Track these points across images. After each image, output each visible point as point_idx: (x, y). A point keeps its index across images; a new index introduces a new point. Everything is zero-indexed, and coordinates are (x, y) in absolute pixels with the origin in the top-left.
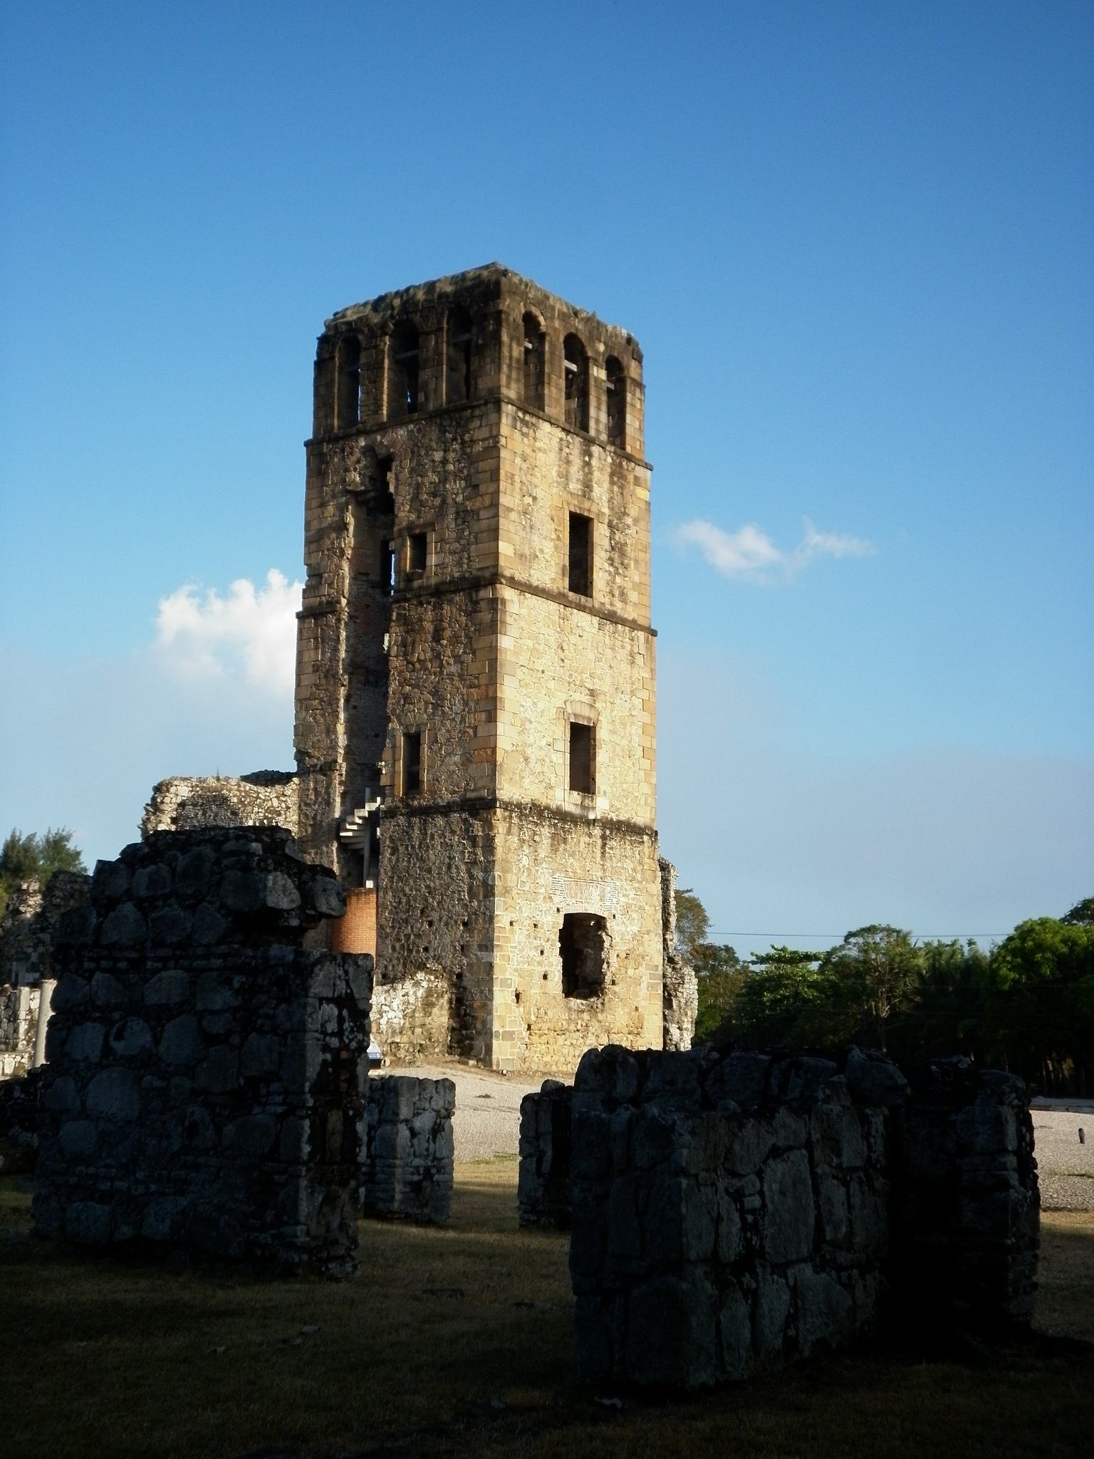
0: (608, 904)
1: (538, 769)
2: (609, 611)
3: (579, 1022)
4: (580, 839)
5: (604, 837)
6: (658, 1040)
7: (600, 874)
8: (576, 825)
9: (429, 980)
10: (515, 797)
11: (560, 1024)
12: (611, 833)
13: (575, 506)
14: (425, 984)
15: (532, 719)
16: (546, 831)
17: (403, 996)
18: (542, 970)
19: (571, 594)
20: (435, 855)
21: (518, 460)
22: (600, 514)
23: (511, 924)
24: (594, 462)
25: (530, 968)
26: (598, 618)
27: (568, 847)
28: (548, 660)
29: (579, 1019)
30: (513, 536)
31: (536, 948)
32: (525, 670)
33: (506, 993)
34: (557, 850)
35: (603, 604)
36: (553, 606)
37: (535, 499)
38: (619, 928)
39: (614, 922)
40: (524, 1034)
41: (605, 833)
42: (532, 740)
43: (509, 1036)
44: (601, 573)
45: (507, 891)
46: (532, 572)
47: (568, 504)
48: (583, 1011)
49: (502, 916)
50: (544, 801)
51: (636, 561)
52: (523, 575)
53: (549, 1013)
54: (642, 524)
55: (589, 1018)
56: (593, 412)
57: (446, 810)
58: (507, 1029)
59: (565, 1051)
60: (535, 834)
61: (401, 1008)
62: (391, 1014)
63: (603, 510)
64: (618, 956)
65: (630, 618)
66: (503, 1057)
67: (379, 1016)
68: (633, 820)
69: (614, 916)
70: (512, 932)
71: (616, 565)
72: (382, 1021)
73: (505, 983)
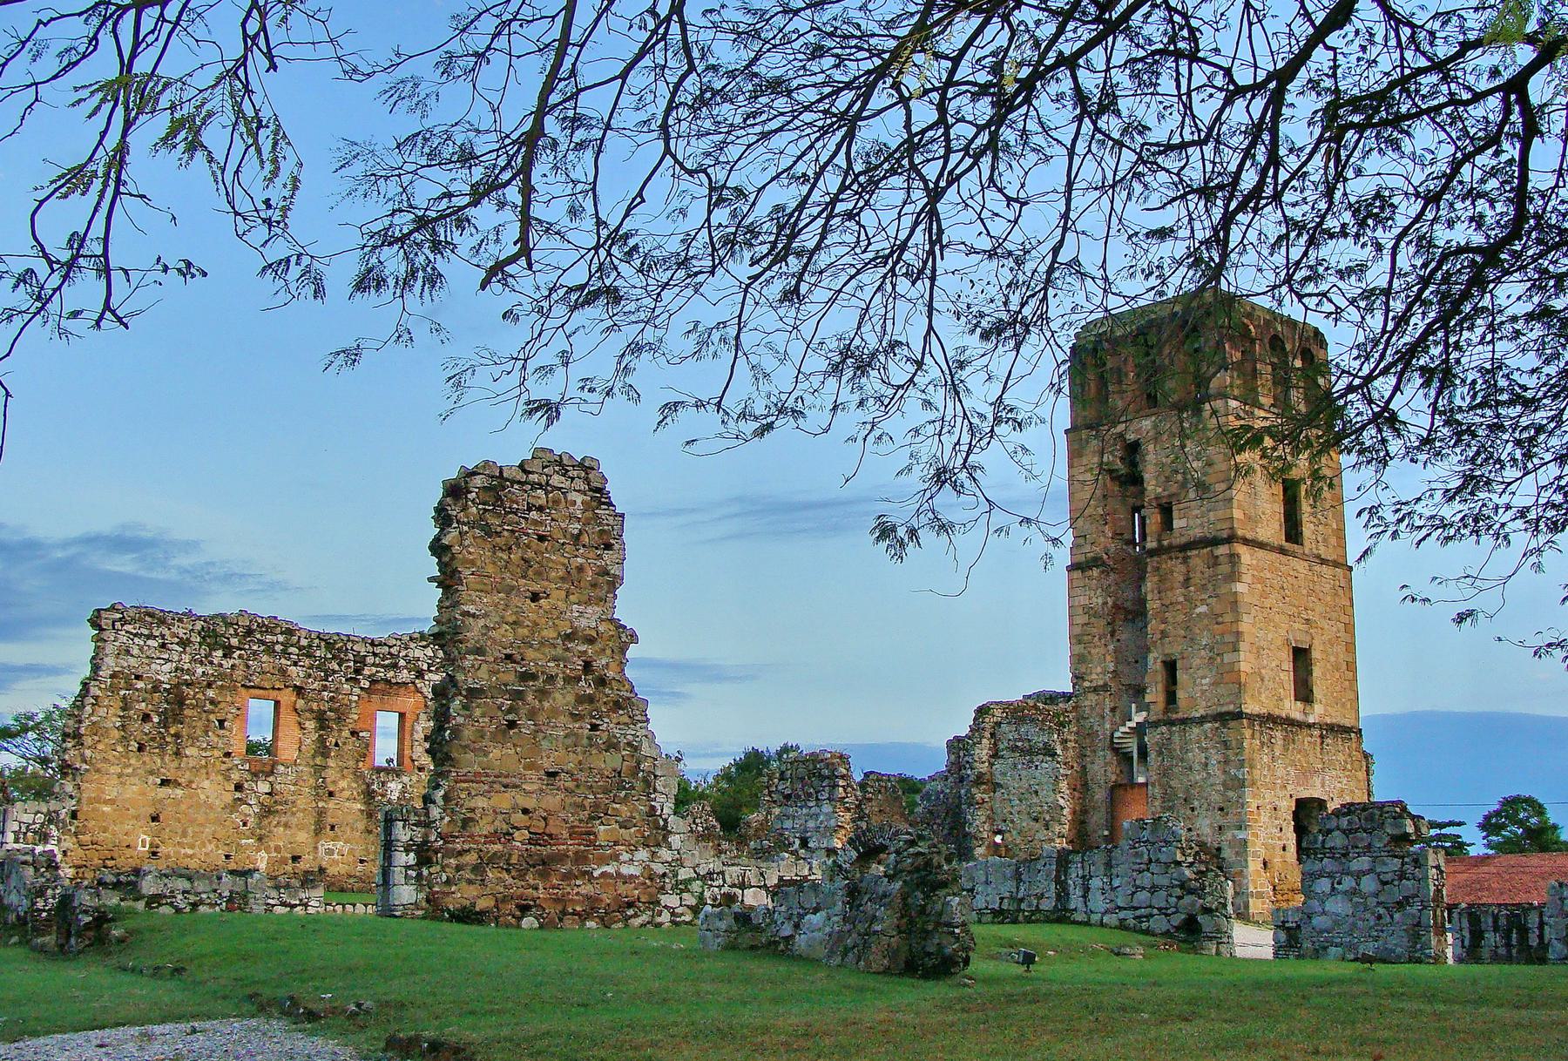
4: (1306, 740)
5: (1322, 736)
16: (1278, 734)
20: (1195, 756)
36: (1274, 556)
43: (1260, 895)
45: (1253, 783)
50: (1277, 712)
57: (1202, 720)
70: (1259, 815)
73: (1255, 854)
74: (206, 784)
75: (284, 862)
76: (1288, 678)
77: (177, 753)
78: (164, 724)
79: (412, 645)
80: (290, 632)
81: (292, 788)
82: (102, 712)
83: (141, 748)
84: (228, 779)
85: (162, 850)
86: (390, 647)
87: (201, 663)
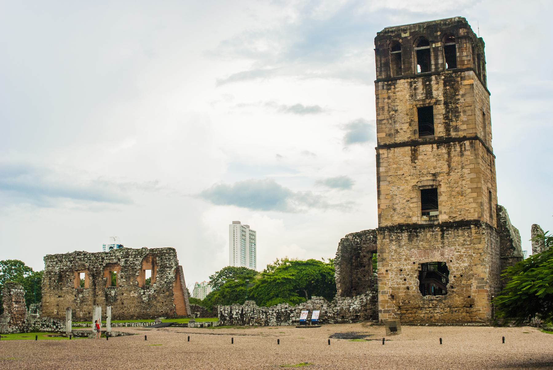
0: (446, 257)
1: (402, 211)
2: (446, 138)
3: (431, 304)
5: (443, 231)
6: (485, 309)
7: (441, 245)
8: (424, 229)
9: (373, 293)
10: (389, 225)
11: (417, 306)
12: (447, 227)
13: (420, 105)
14: (371, 295)
15: (397, 194)
16: (405, 235)
17: (361, 299)
18: (406, 286)
19: (419, 140)
21: (386, 100)
22: (437, 102)
23: (387, 271)
24: (433, 83)
25: (398, 286)
26: (436, 144)
27: (419, 238)
28: (407, 169)
29: (430, 303)
30: (384, 129)
31: (401, 279)
32: (392, 177)
33: (385, 296)
34: (411, 241)
35: (443, 136)
37: (396, 111)
38: (455, 265)
39: (451, 264)
40: (396, 310)
41: (443, 229)
42: (397, 201)
43: (388, 311)
44: (440, 125)
45: (383, 260)
46: (396, 139)
47: (416, 105)
48: (432, 300)
49: (381, 269)
51: (464, 112)
52: (391, 142)
53: (411, 302)
54: (467, 95)
55: (437, 302)
56: (433, 62)
58: (386, 309)
59: (422, 315)
60: (399, 236)
61: (359, 303)
62: (355, 306)
63: (440, 99)
64: (455, 277)
65: (461, 137)
66: (385, 319)
67: (348, 307)
68: (467, 219)
69: (451, 261)
70: (387, 274)
71: (450, 118)
72: (350, 309)
73: (384, 293)
74: (68, 296)
75: (86, 314)
76: (416, 206)
77: (61, 289)
78: (58, 282)
79: (116, 252)
80: (85, 254)
81: (88, 295)
82: (45, 281)
83: (54, 289)
84: (72, 294)
85: (59, 313)
86: (111, 254)
87: (65, 266)
